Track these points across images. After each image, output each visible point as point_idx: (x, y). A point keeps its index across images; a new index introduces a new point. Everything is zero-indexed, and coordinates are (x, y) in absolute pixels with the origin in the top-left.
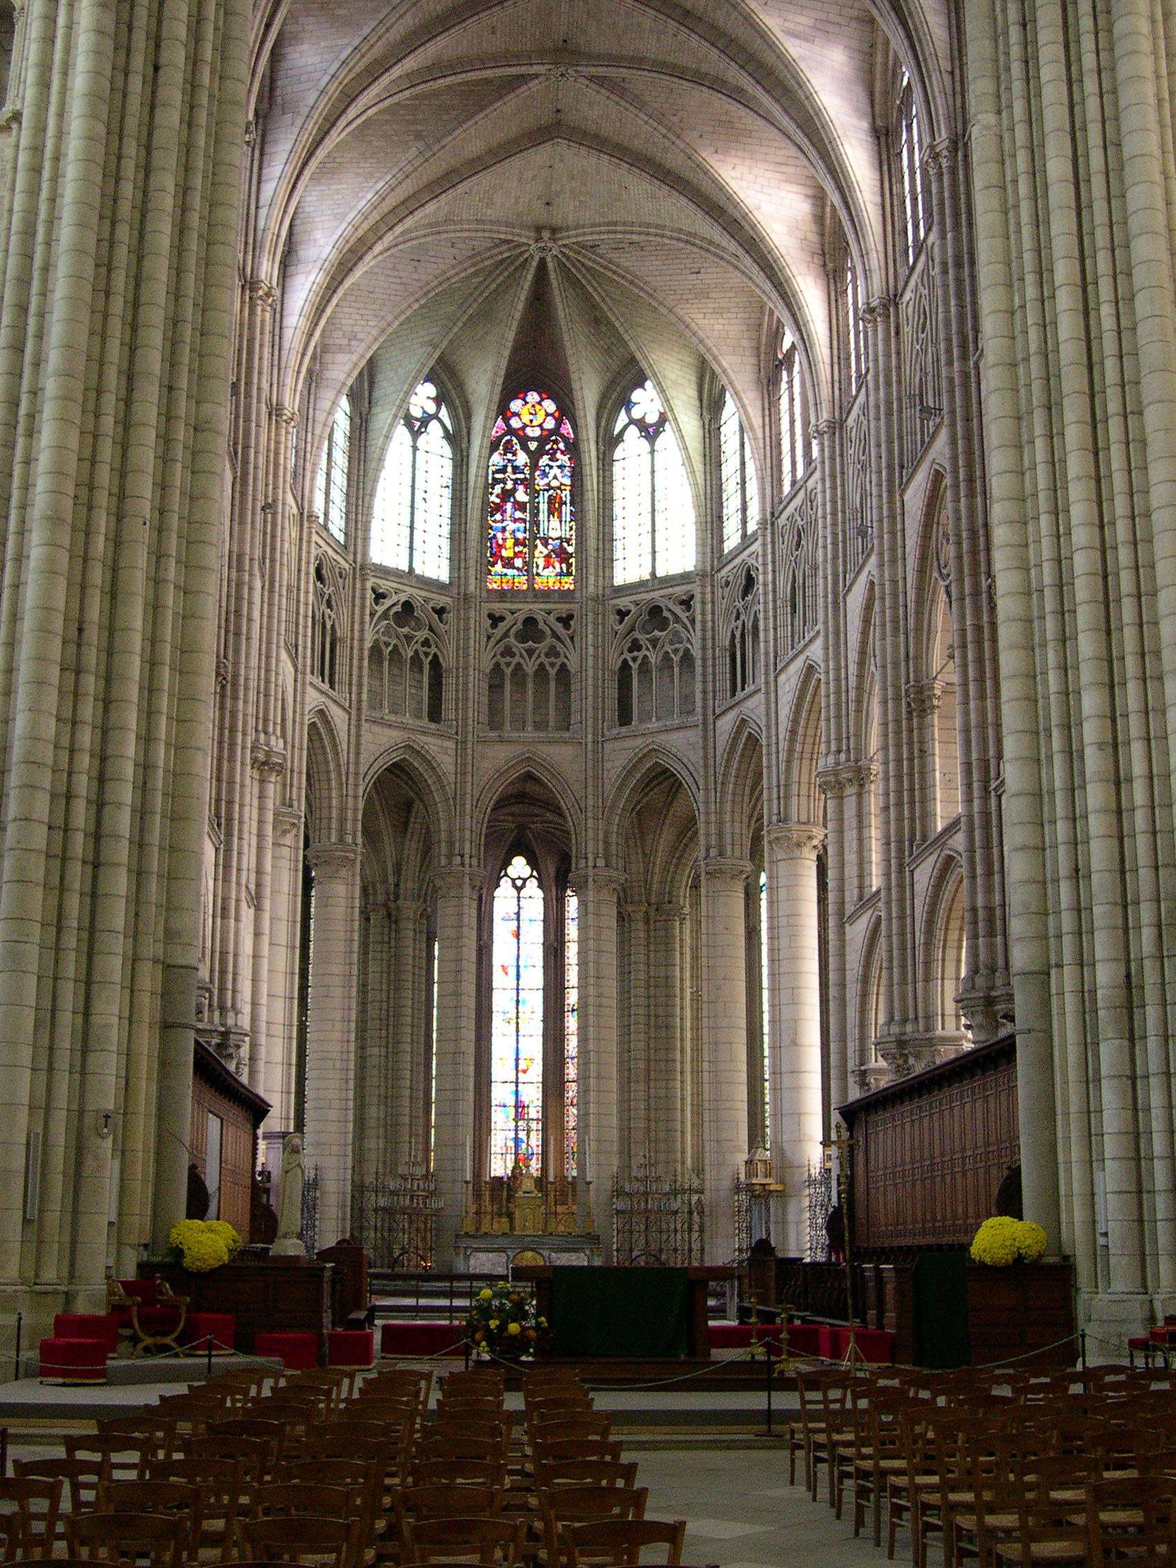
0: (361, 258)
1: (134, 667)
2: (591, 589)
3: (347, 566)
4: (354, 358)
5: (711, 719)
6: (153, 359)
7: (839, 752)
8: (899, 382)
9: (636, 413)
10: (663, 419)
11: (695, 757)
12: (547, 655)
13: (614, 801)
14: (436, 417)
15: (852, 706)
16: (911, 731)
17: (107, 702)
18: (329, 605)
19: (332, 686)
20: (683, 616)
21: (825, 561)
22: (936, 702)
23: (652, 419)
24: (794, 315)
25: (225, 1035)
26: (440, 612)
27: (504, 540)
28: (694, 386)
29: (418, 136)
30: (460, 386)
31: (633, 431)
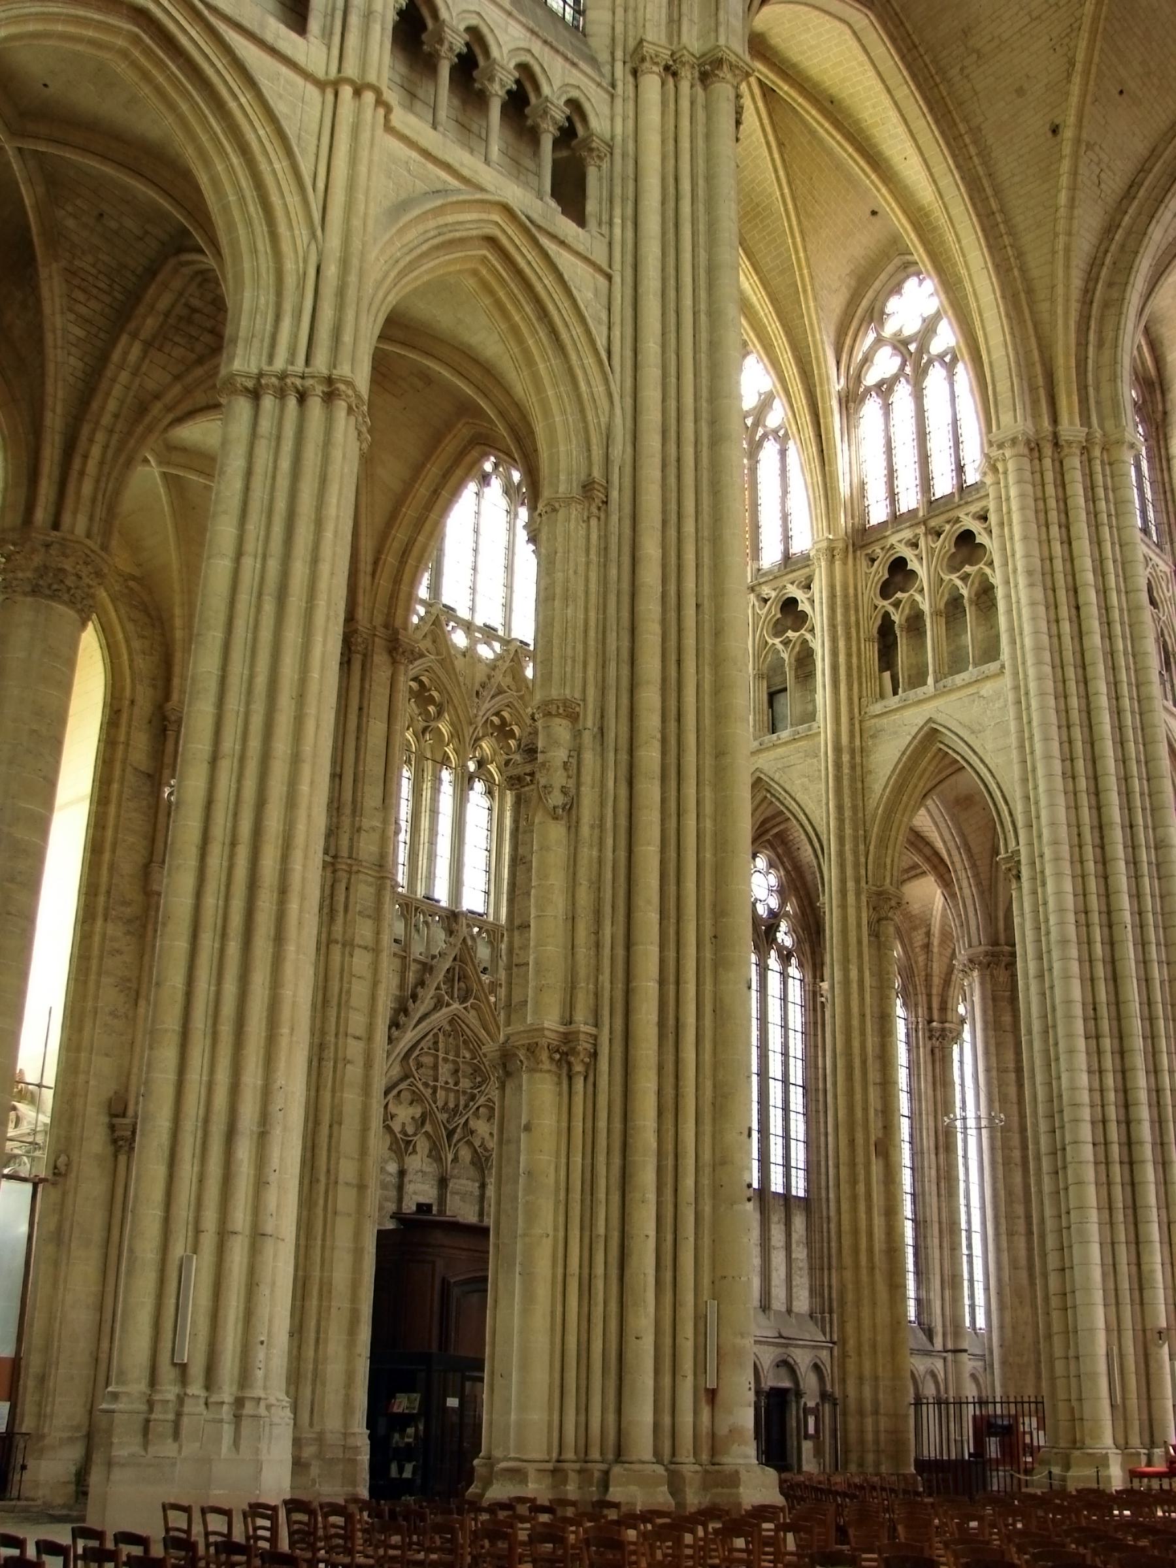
1: (1136, 1026)
6: (1115, 814)
17: (1122, 1053)
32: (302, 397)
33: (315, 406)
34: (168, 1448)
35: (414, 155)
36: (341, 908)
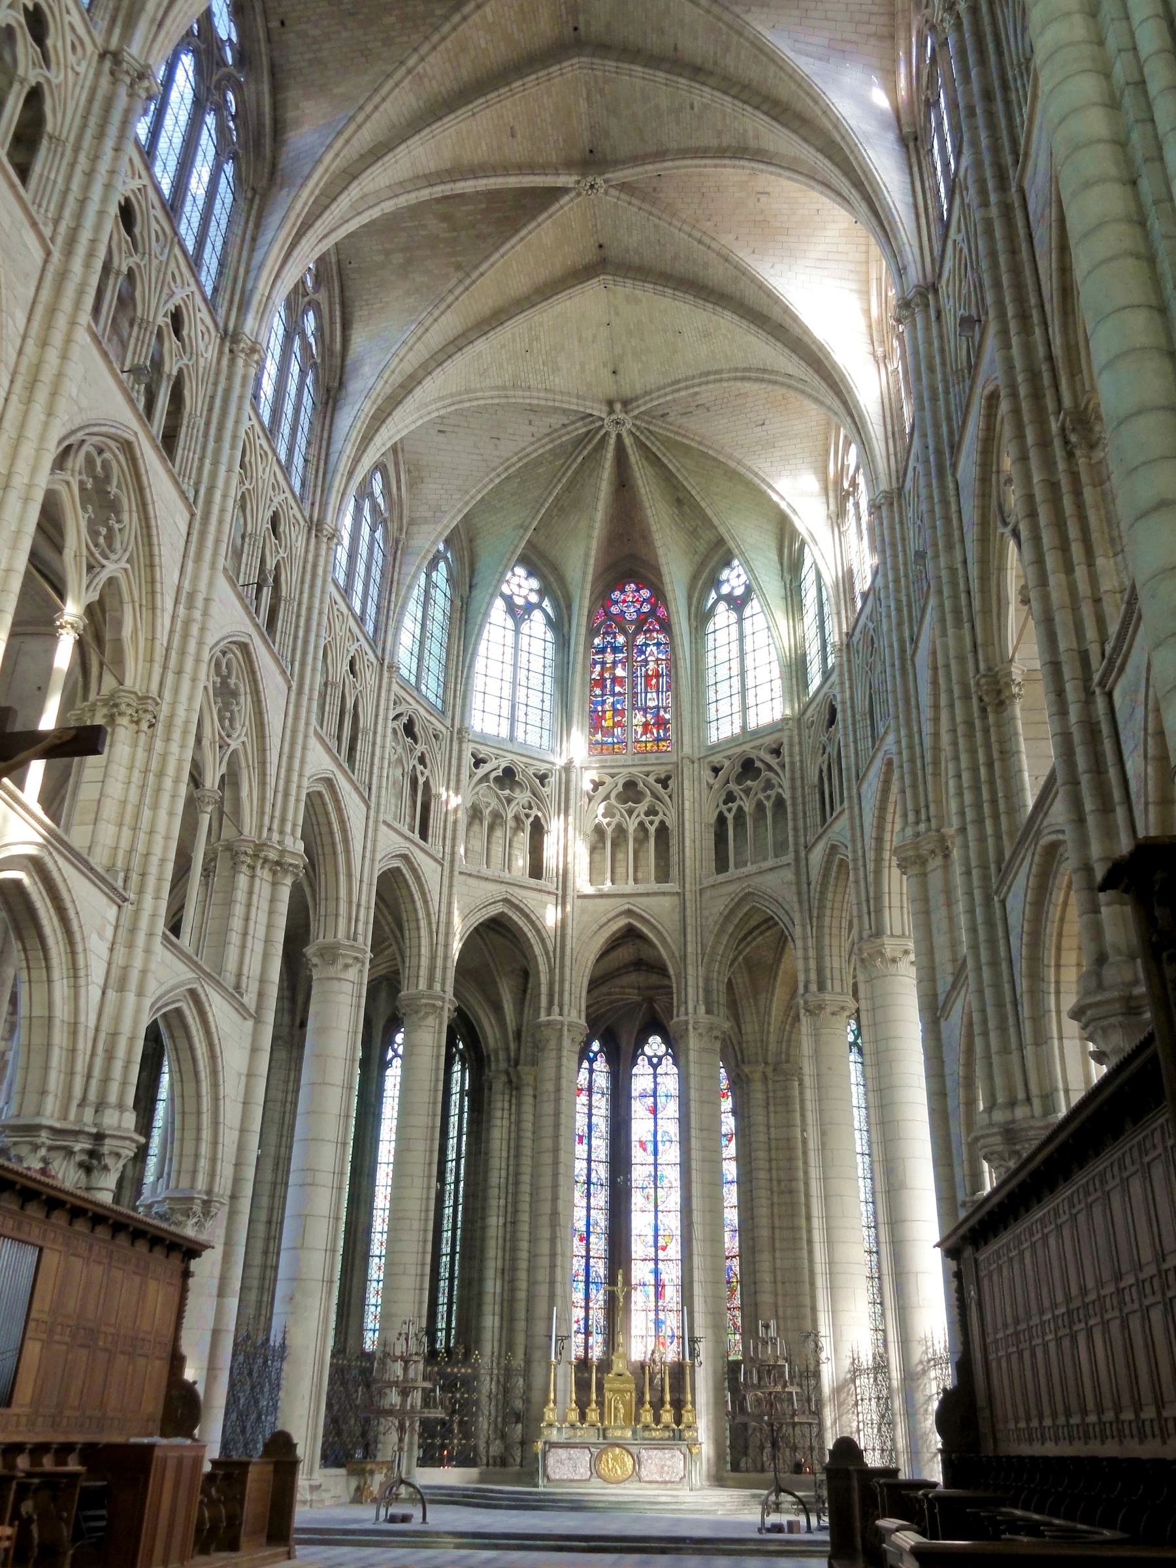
0: (410, 392)
2: (687, 749)
3: (444, 730)
4: (439, 528)
5: (803, 854)
7: (917, 823)
8: (943, 364)
9: (725, 589)
10: (749, 590)
11: (790, 897)
12: (647, 814)
13: (713, 948)
14: (539, 606)
15: (929, 769)
16: (986, 731)
18: (422, 760)
19: (424, 835)
20: (773, 761)
21: (890, 631)
22: (1015, 690)
23: (739, 592)
24: (845, 403)
25: (99, 1137)
26: (543, 778)
27: (604, 712)
28: (773, 544)
29: (458, 267)
30: (561, 579)
31: (722, 607)
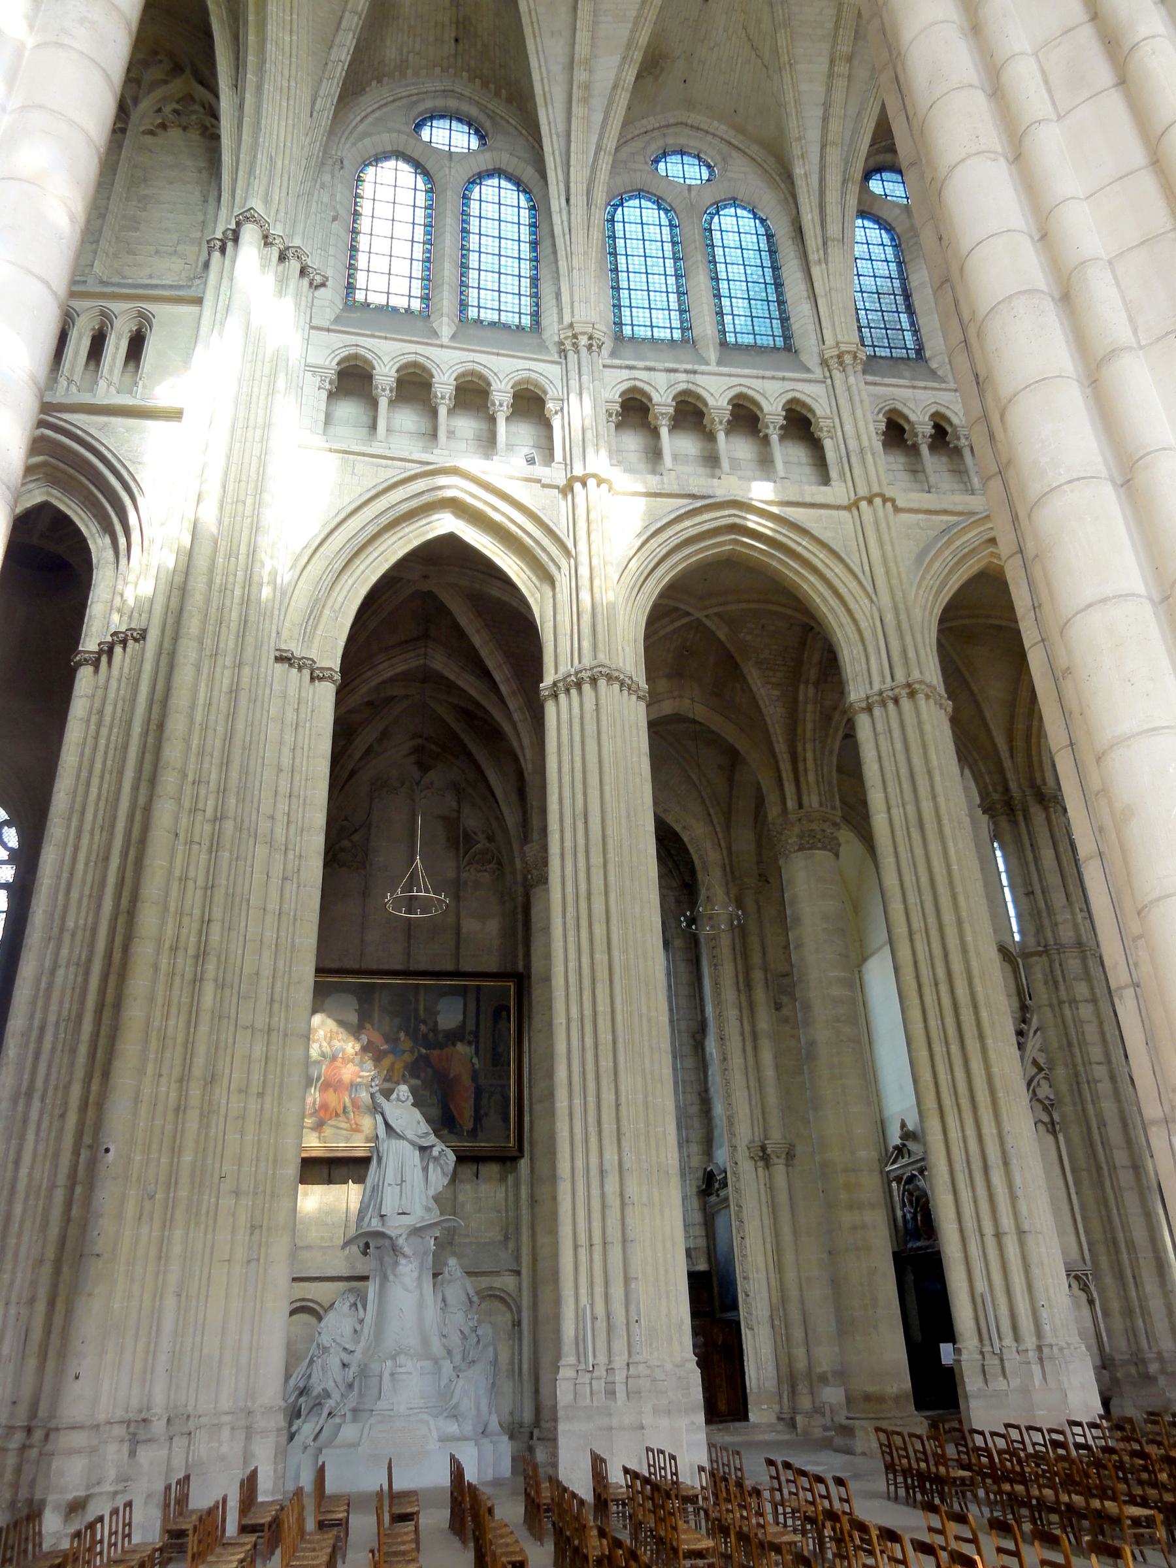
32: (896, 701)
33: (905, 703)
34: (1000, 1384)
35: (921, 516)
36: (1060, 979)
